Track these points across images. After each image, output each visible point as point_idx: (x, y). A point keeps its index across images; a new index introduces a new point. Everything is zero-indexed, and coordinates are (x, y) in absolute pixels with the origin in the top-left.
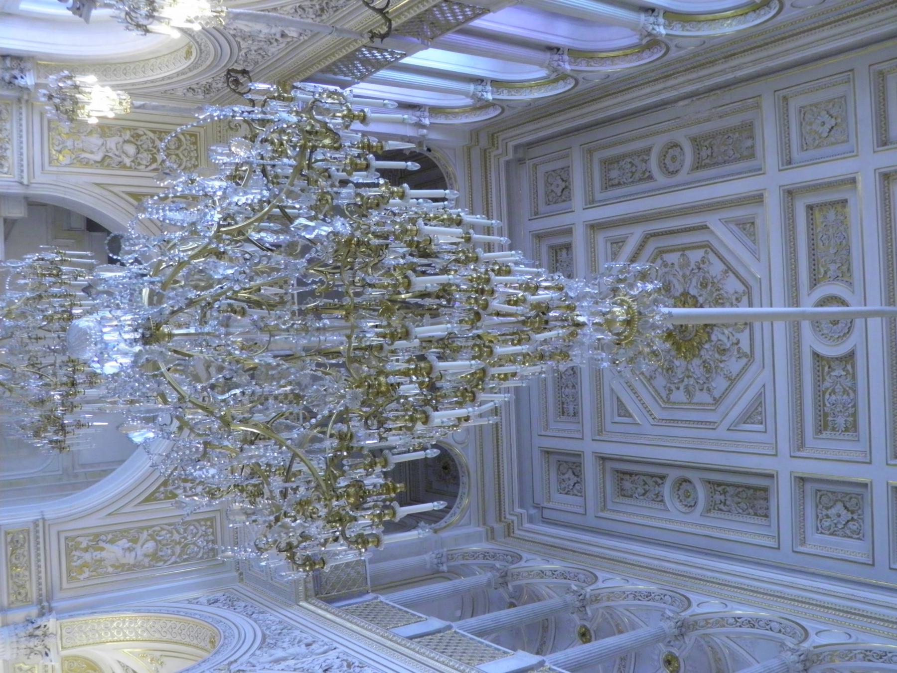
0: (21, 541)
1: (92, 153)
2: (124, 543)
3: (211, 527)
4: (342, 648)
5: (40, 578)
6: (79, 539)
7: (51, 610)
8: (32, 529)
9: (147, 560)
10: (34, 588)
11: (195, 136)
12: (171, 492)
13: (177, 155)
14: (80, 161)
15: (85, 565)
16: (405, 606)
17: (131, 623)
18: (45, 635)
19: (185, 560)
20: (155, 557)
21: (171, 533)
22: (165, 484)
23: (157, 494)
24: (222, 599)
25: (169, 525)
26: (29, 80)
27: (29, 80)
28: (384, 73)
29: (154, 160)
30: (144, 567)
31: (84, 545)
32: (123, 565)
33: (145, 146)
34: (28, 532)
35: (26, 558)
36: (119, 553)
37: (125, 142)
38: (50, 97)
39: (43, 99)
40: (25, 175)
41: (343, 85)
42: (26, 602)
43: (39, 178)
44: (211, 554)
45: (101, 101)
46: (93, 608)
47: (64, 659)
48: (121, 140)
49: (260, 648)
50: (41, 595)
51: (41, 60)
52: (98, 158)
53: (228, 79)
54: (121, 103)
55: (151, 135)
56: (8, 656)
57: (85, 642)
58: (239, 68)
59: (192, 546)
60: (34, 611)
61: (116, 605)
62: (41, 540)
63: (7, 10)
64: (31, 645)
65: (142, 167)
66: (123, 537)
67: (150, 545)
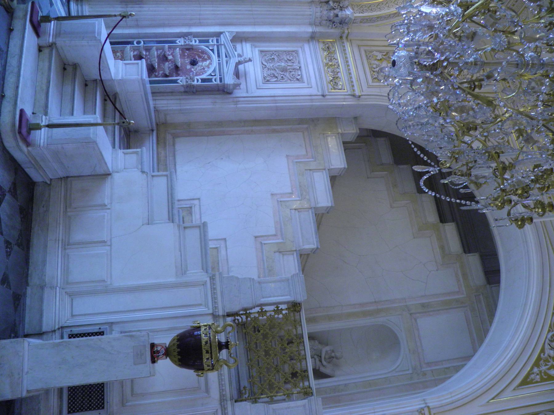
22: (537, 364)
23: (532, 376)
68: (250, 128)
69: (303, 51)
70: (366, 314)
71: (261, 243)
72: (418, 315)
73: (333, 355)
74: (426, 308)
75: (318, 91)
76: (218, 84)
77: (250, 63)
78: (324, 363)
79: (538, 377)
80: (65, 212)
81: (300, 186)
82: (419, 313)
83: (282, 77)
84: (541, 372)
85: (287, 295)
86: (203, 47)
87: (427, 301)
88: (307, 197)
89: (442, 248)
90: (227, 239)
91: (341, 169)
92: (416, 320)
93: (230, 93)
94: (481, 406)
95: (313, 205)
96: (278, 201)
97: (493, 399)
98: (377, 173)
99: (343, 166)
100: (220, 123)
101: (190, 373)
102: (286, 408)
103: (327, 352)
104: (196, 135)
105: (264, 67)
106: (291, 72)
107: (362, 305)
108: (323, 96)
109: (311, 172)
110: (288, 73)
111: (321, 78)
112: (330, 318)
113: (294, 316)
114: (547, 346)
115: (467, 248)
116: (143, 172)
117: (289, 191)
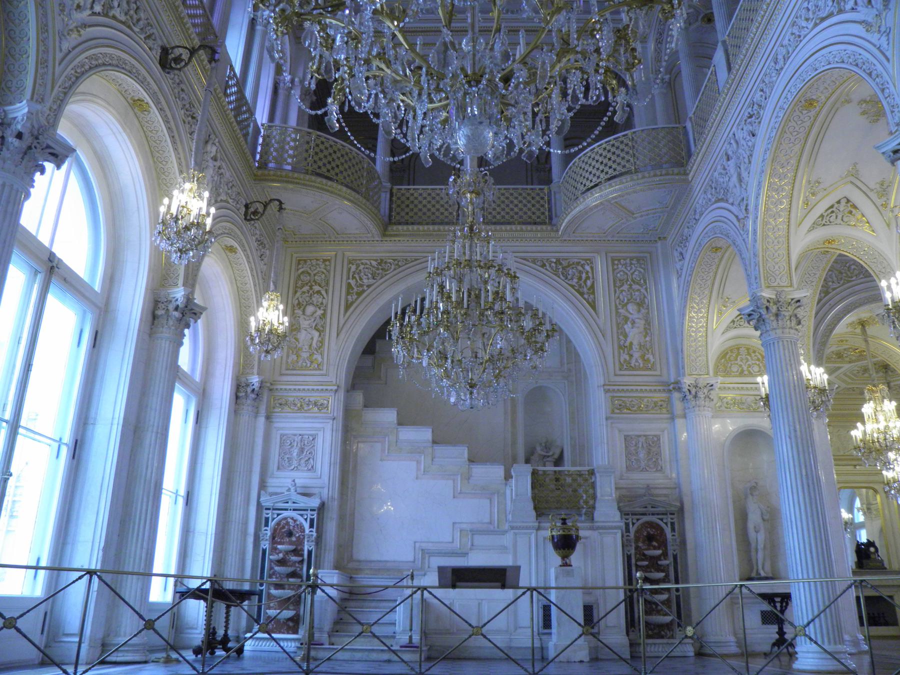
0: (621, 402)
1: (312, 339)
2: (628, 327)
3: (619, 260)
4: (734, 129)
5: (650, 391)
6: (622, 361)
7: (677, 382)
8: (611, 394)
9: (643, 311)
10: (659, 395)
11: (299, 260)
12: (589, 289)
13: (315, 275)
14: (320, 348)
15: (643, 357)
16: (698, 94)
17: (693, 322)
18: (696, 387)
19: (645, 281)
20: (641, 304)
21: (622, 291)
22: (582, 294)
24: (679, 249)
25: (615, 292)
26: (255, 380)
27: (255, 380)
28: (248, 93)
29: (319, 292)
30: (648, 313)
31: (627, 357)
32: (645, 329)
33: (308, 299)
34: (613, 397)
36: (635, 330)
37: (304, 314)
38: (267, 352)
39: (269, 357)
40: (329, 388)
41: (257, 131)
42: (669, 401)
43: (332, 378)
44: (642, 262)
45: (271, 314)
46: (678, 353)
47: (716, 374)
48: (302, 317)
49: (727, 201)
50: (664, 390)
51: (239, 364)
52: (316, 334)
53: (252, 219)
54: (272, 300)
55: (298, 294)
56: (710, 414)
57: (705, 358)
58: (244, 209)
60: (676, 395)
61: (677, 334)
62: (621, 388)
63: (201, 391)
64: (702, 396)
65: (324, 301)
66: (623, 327)
67: (631, 308)
69: (282, 428)
70: (514, 412)
77: (296, 481)
78: (551, 453)
80: (453, 633)
86: (272, 524)
95: (430, 444)
101: (579, 547)
104: (351, 540)
105: (296, 469)
107: (506, 413)
111: (316, 418)
112: (514, 443)
116: (425, 575)
117: (415, 463)
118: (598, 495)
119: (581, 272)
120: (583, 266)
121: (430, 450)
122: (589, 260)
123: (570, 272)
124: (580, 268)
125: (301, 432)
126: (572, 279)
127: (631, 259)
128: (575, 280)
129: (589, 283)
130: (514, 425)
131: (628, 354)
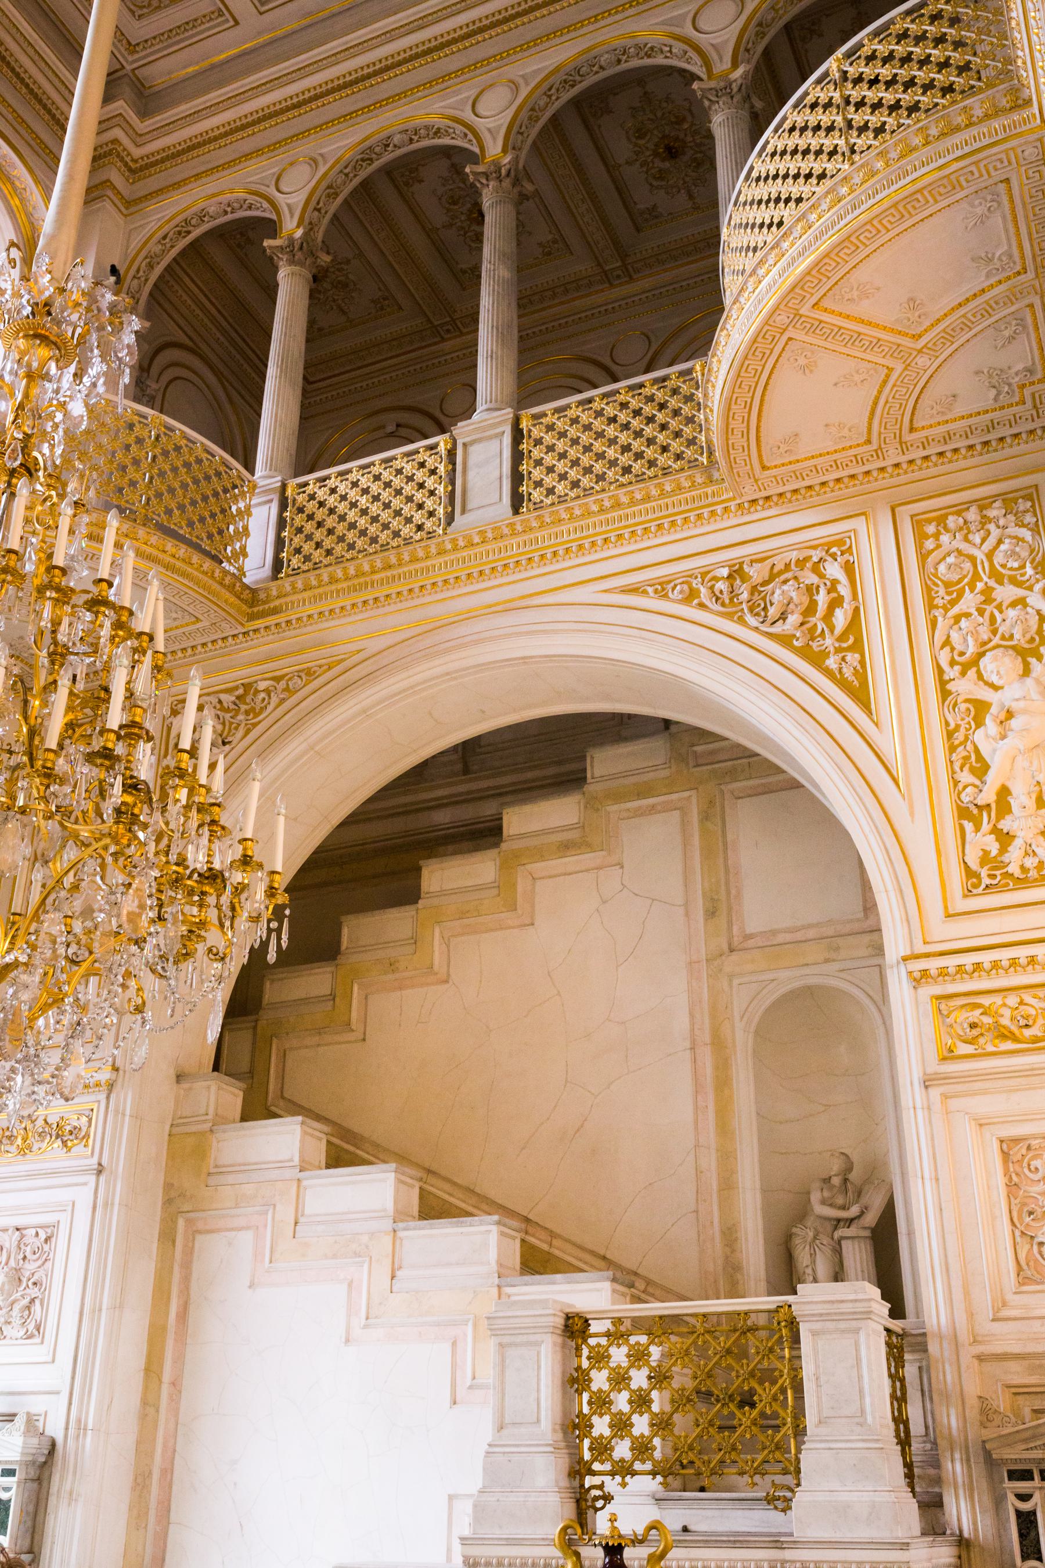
2: (984, 738)
3: (941, 521)
22: (817, 660)
23: (848, 672)
25: (933, 624)
35: (1028, 999)
59: (999, 558)
68: (165, 1389)
70: (723, 1082)
71: (470, 1387)
72: (735, 929)
73: (836, 1181)
74: (718, 906)
75: (85, 1184)
76: (19, 1483)
79: (849, 658)
81: (335, 1256)
82: (730, 923)
83: (35, 1284)
84: (838, 650)
85: (539, 1353)
87: (700, 902)
88: (365, 1239)
89: (566, 847)
90: (452, 1492)
91: (304, 1133)
92: (750, 937)
93: (53, 1444)
94: (912, 814)
95: (387, 1224)
96: (366, 1327)
97: (895, 781)
98: (354, 1015)
99: (298, 1129)
100: (140, 1482)
102: (818, 1386)
103: (823, 1202)
106: (25, 1258)
108: (99, 1172)
109: (302, 1220)
110: (27, 1266)
111: (54, 1173)
112: (728, 1185)
113: (596, 1335)
114: (777, 629)
115: (572, 780)
118: (811, 1419)
119: (811, 590)
120: (816, 569)
121: (388, 1240)
122: (840, 543)
123: (777, 597)
124: (812, 579)
125: (20, 1221)
126: (783, 617)
127: (983, 505)
128: (793, 619)
129: (841, 618)
130: (724, 1128)
131: (996, 831)
